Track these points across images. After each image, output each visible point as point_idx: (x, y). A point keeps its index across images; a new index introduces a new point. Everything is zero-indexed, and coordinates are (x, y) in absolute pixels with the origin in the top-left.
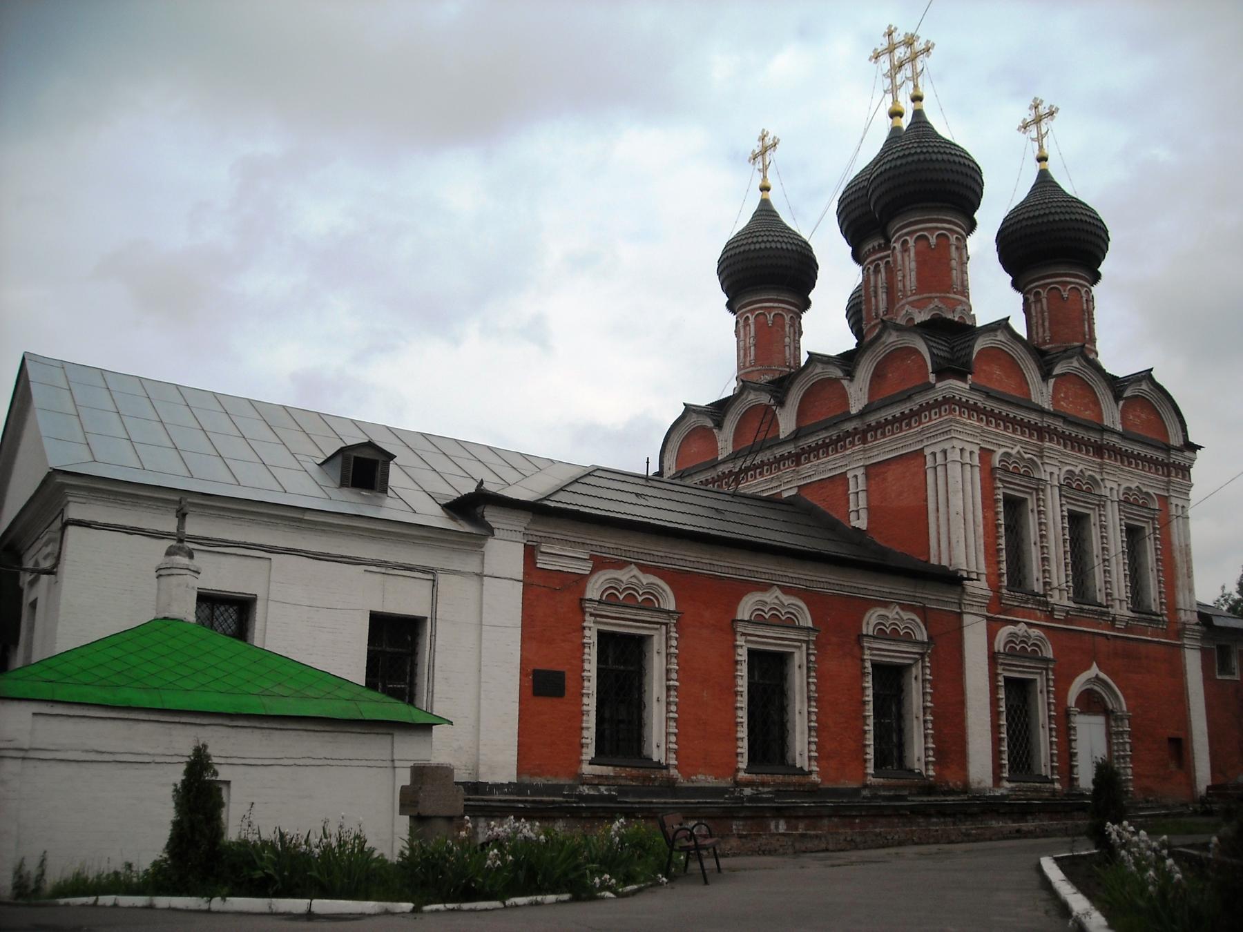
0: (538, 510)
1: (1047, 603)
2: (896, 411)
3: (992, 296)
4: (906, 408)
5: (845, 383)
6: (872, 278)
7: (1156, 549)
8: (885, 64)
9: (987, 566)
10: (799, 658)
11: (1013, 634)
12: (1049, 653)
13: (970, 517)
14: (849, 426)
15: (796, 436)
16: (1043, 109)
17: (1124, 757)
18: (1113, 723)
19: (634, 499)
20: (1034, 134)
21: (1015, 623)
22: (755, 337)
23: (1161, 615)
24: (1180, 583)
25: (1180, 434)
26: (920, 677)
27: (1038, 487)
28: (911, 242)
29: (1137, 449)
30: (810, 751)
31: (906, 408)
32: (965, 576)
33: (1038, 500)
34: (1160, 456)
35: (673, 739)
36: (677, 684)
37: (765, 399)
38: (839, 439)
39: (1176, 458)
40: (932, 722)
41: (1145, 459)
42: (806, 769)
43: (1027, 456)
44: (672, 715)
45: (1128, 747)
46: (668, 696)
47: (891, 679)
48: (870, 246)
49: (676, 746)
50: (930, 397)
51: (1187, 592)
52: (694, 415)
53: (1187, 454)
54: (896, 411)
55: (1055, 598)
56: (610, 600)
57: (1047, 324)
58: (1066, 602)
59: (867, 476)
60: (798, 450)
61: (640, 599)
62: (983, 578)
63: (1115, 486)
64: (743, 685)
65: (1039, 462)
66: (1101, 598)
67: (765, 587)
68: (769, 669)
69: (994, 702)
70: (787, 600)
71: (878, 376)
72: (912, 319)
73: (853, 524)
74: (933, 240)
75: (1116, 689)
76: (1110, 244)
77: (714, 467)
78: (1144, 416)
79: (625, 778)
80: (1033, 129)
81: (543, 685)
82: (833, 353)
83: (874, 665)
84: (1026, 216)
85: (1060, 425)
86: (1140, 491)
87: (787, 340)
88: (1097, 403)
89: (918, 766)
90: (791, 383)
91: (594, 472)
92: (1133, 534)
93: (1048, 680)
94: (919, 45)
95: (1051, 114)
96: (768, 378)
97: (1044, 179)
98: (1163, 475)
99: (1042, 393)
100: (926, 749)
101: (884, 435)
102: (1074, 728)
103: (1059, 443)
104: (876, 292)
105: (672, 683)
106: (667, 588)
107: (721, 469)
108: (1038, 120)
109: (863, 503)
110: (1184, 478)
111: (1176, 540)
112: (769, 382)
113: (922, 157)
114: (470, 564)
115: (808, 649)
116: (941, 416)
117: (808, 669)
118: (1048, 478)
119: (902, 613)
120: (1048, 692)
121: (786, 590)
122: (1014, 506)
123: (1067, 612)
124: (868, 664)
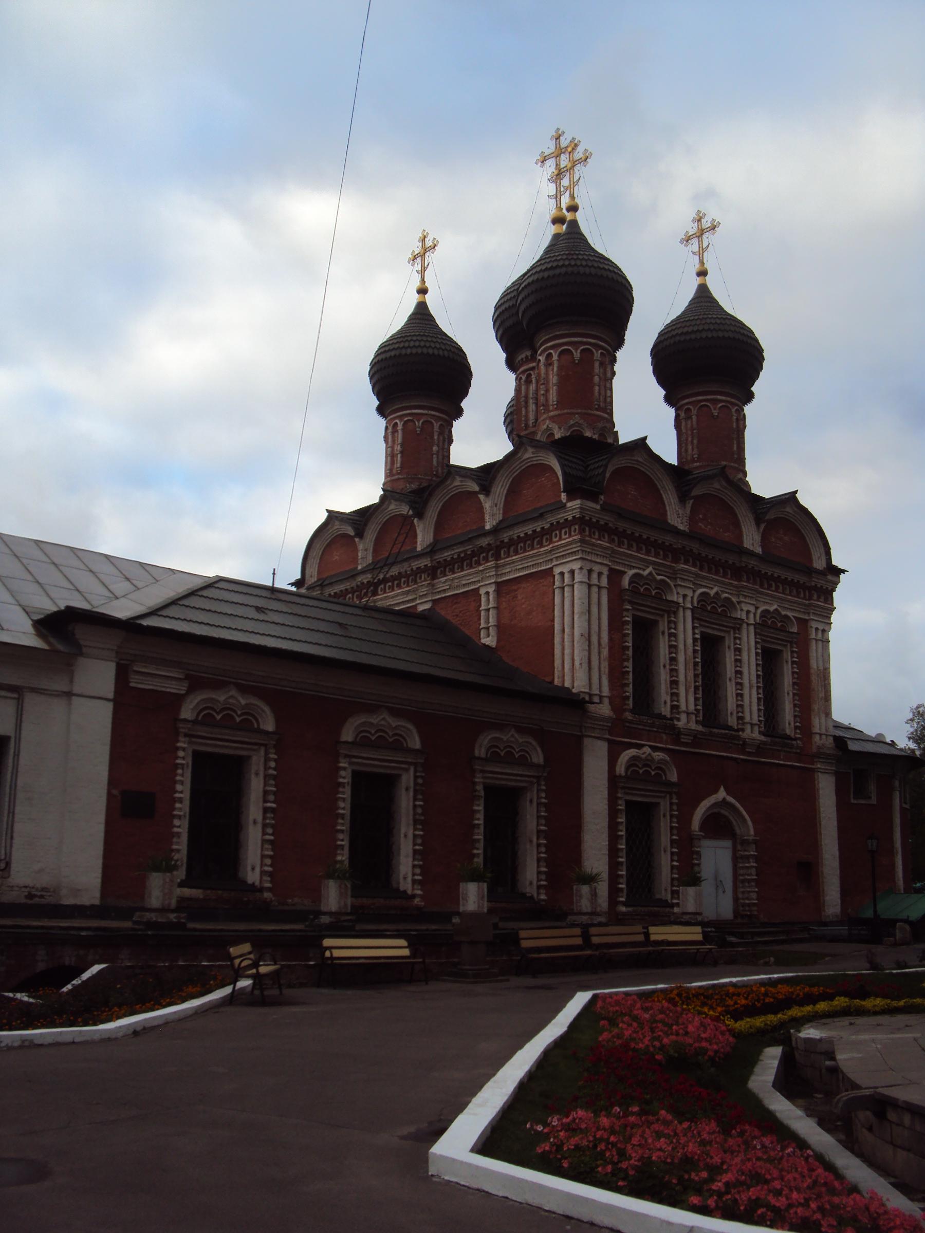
0: (131, 628)
1: (674, 727)
2: (528, 529)
3: (641, 411)
4: (538, 526)
5: (481, 497)
6: (523, 388)
7: (793, 673)
8: (550, 167)
9: (611, 689)
10: (407, 779)
11: (634, 758)
12: (673, 777)
13: (595, 639)
14: (484, 542)
15: (431, 550)
16: (706, 223)
17: (749, 881)
18: (739, 847)
19: (253, 614)
20: (696, 249)
21: (639, 747)
22: (402, 445)
23: (796, 739)
24: (816, 707)
25: (824, 558)
26: (535, 800)
27: (672, 609)
28: (555, 357)
29: (777, 572)
30: (414, 875)
31: (538, 526)
32: (587, 698)
33: (669, 622)
34: (802, 579)
35: (268, 861)
36: (274, 805)
37: (405, 509)
38: (474, 554)
39: (820, 582)
40: (545, 845)
41: (785, 582)
42: (409, 892)
43: (659, 578)
44: (267, 837)
45: (753, 871)
46: (264, 818)
47: (504, 804)
48: (523, 356)
49: (270, 869)
50: (562, 516)
51: (823, 716)
52: (337, 523)
53: (830, 577)
54: (528, 529)
55: (682, 722)
56: (205, 719)
57: (695, 442)
58: (693, 726)
59: (498, 592)
60: (434, 563)
61: (238, 720)
62: (606, 701)
63: (752, 609)
64: (344, 807)
65: (672, 584)
66: (732, 721)
67: (372, 709)
68: (375, 792)
69: (613, 826)
70: (394, 722)
71: (513, 492)
72: (552, 434)
73: (483, 641)
74: (577, 355)
75: (744, 813)
76: (765, 364)
77: (353, 576)
78: (786, 538)
80: (695, 241)
82: (474, 465)
83: (487, 788)
84: (680, 331)
85: (695, 547)
86: (779, 613)
87: (435, 448)
88: (737, 525)
89: (531, 891)
90: (430, 495)
91: (218, 582)
92: (769, 660)
93: (671, 804)
94: (579, 154)
95: (713, 228)
96: (414, 486)
97: (703, 294)
98: (804, 598)
99: (677, 515)
100: (539, 873)
101: (516, 553)
102: (698, 853)
103: (694, 565)
104: (526, 402)
105: (269, 805)
106: (267, 709)
107: (359, 579)
108: (701, 233)
109: (492, 621)
110: (826, 601)
111: (813, 664)
112: (413, 492)
113: (570, 269)
115: (416, 771)
116: (570, 536)
117: (416, 791)
118: (681, 600)
119: (516, 735)
120: (672, 816)
121: (395, 713)
122: (645, 631)
123: (695, 737)
124: (480, 788)
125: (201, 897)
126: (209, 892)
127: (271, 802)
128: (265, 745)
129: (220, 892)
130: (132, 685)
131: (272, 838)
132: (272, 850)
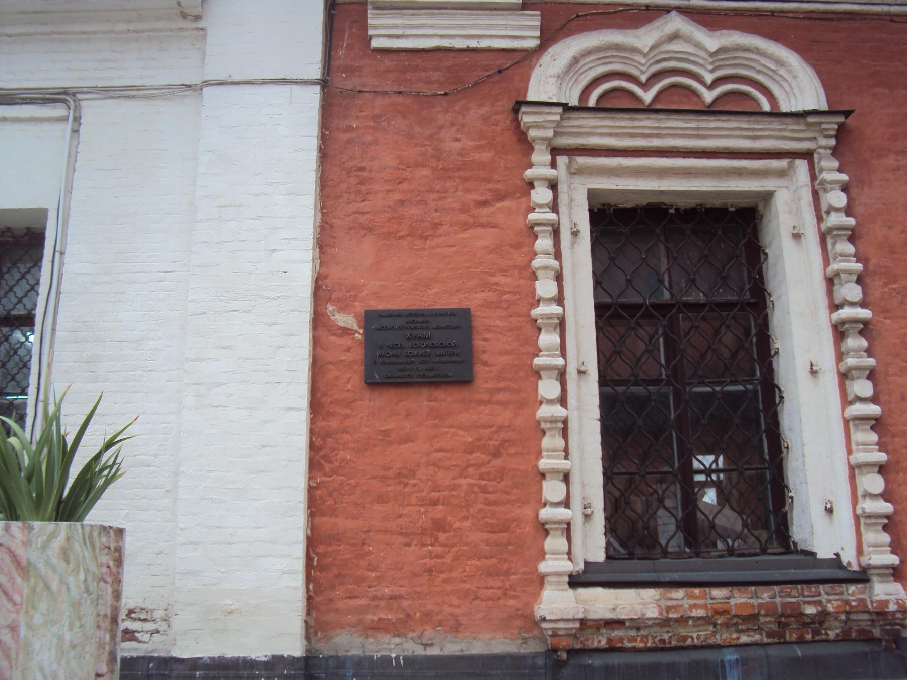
35: (876, 483)
46: (840, 356)
79: (707, 620)
81: (403, 354)
114: (171, 66)
125: (652, 613)
126: (679, 594)
127: (852, 304)
128: (808, 155)
129: (717, 593)
130: (376, 43)
131: (874, 410)
132: (882, 446)
